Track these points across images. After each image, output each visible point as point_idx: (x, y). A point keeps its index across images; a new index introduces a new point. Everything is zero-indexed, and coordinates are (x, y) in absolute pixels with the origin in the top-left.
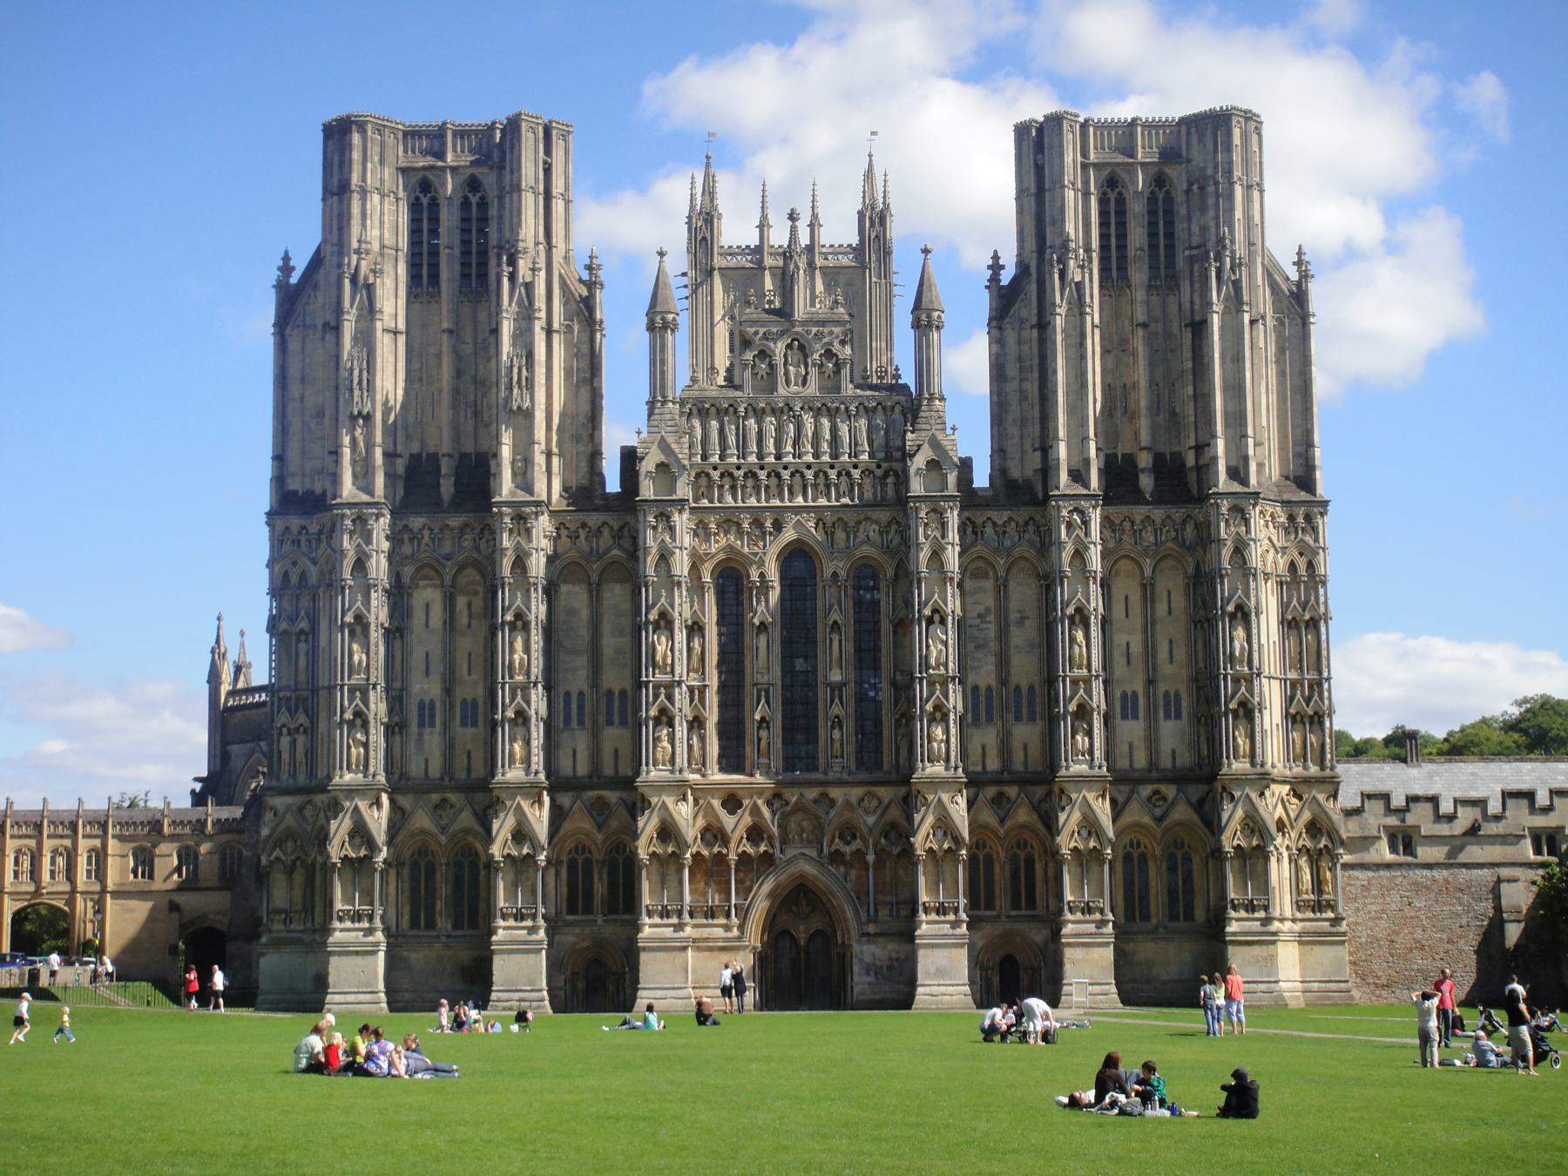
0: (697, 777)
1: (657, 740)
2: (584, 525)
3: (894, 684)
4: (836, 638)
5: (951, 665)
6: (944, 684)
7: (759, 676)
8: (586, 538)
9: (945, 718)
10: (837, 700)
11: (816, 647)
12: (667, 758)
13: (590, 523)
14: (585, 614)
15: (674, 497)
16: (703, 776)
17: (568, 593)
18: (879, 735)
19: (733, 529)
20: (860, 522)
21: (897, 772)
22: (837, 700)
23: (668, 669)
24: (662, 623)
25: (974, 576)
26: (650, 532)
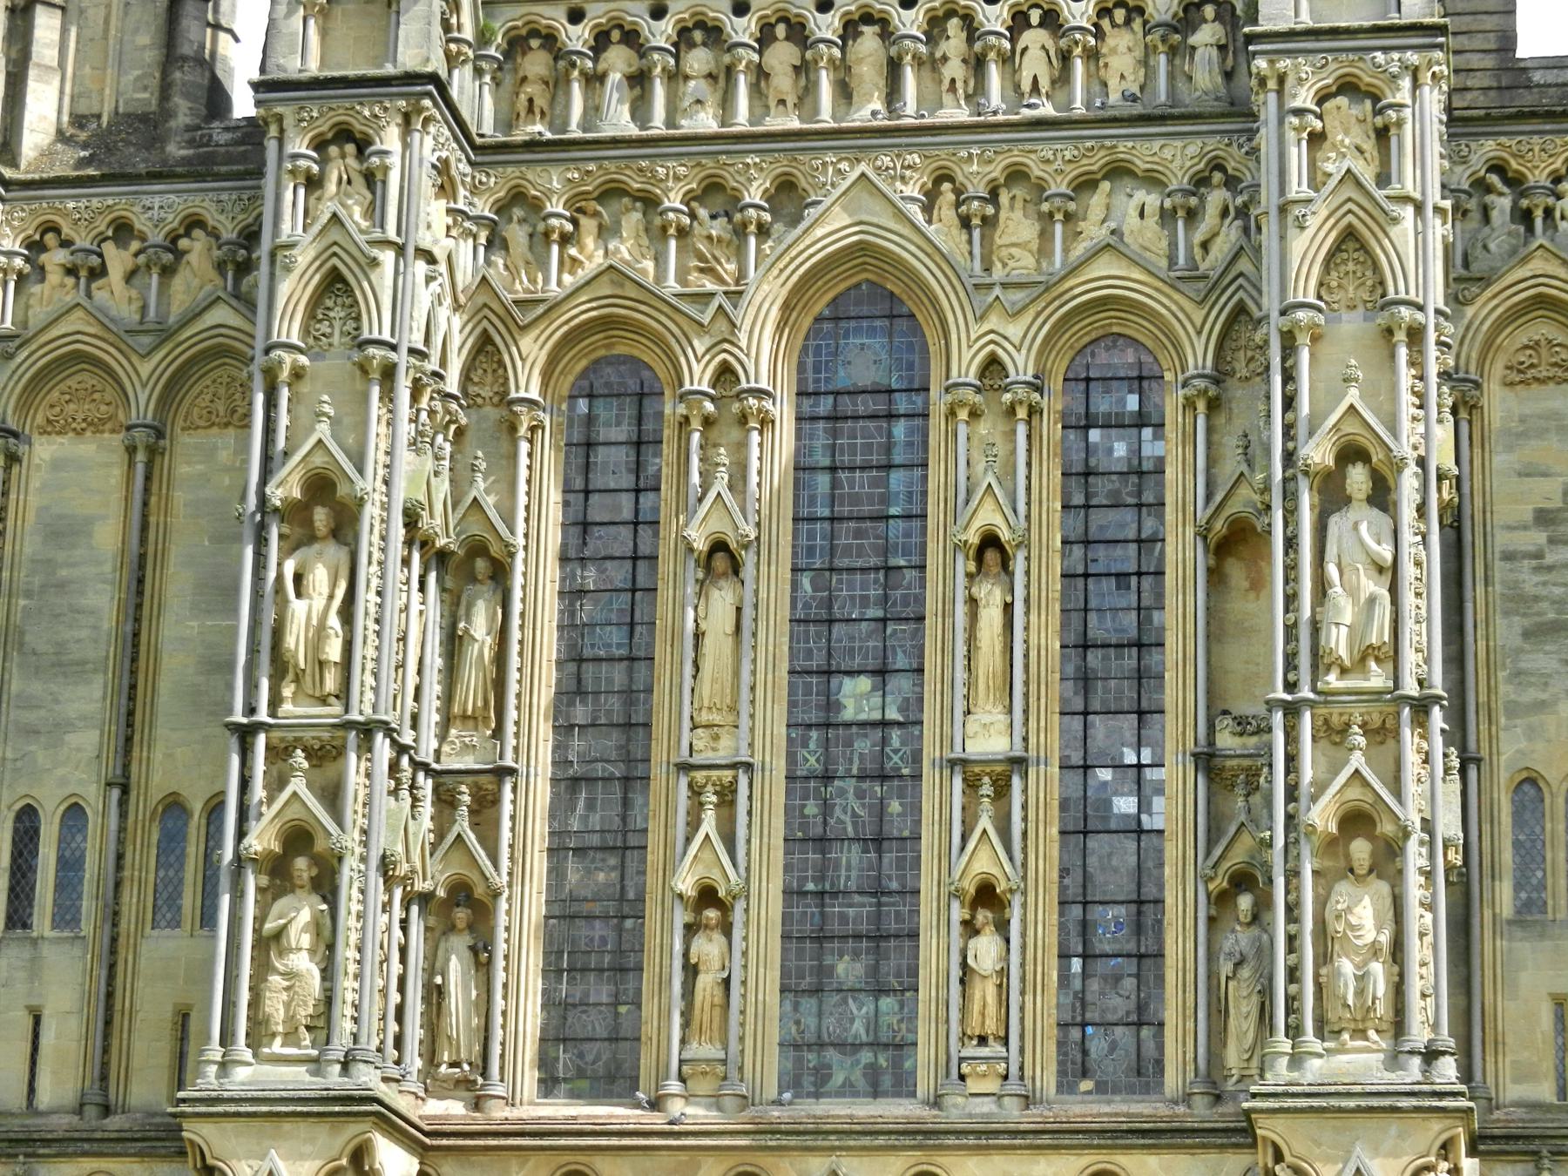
0: (453, 1109)
1: (270, 943)
2: (122, 231)
3: (1207, 761)
4: (991, 595)
5: (1410, 658)
6: (1383, 734)
7: (701, 739)
8: (130, 277)
9: (1388, 858)
10: (985, 822)
11: (919, 635)
12: (304, 1012)
13: (140, 223)
14: (108, 537)
15: (389, 70)
16: (477, 1105)
17: (57, 465)
18: (1149, 959)
19: (633, 220)
20: (1085, 185)
21: (1218, 1098)
22: (985, 822)
23: (331, 682)
24: (321, 516)
25: (1521, 376)
26: (292, 197)
